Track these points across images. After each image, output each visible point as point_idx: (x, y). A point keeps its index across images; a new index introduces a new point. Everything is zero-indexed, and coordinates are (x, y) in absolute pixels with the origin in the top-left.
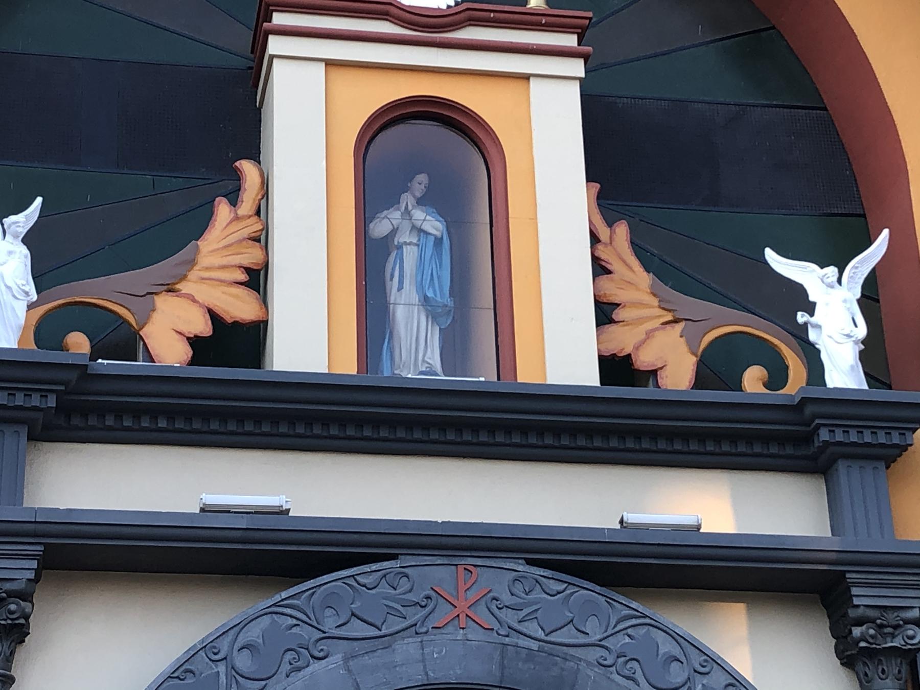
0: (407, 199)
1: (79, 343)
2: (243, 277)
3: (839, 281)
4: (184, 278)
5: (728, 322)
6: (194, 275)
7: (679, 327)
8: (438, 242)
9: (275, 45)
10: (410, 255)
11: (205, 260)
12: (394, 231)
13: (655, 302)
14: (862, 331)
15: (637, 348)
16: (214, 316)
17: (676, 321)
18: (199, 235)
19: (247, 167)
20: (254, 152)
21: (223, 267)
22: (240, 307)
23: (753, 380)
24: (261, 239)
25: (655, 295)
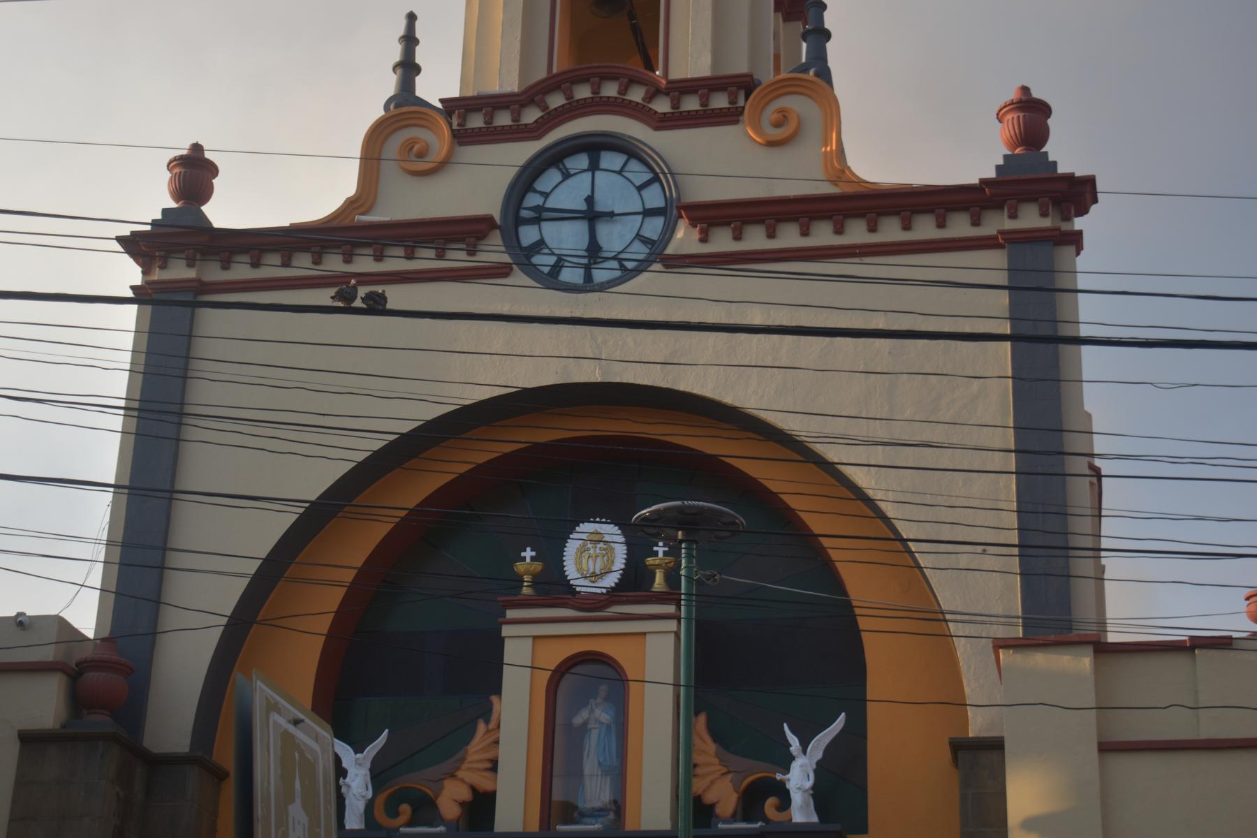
0: (599, 700)
1: (406, 809)
2: (488, 765)
3: (804, 752)
4: (458, 768)
5: (758, 771)
6: (464, 766)
7: (730, 776)
8: (609, 727)
9: (506, 631)
10: (594, 735)
11: (470, 758)
12: (585, 723)
13: (716, 761)
14: (809, 784)
15: (704, 791)
16: (474, 789)
17: (729, 772)
18: (468, 743)
19: (494, 699)
20: (498, 690)
21: (480, 761)
22: (484, 783)
23: (770, 804)
24: (497, 742)
25: (717, 756)
